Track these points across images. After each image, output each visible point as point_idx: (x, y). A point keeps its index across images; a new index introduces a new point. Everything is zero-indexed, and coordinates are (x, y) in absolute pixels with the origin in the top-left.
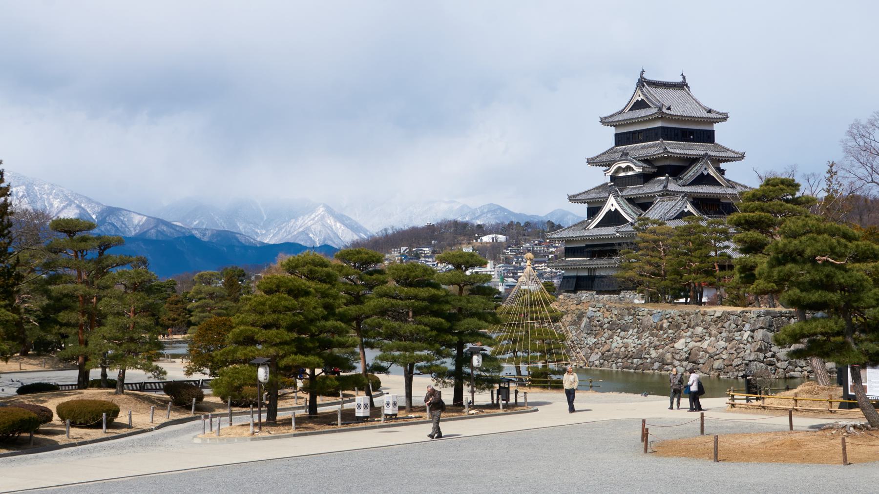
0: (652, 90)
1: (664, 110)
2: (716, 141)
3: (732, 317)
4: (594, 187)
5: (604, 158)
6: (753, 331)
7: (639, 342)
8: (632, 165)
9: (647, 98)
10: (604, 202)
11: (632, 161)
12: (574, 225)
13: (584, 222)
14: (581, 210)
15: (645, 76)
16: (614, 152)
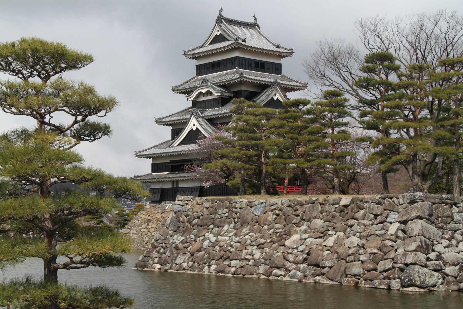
0: (230, 27)
1: (240, 41)
2: (283, 73)
3: (366, 205)
4: (178, 111)
5: (187, 86)
6: (405, 222)
7: (237, 239)
8: (211, 90)
9: (225, 32)
10: (185, 123)
11: (211, 87)
12: (160, 144)
13: (168, 141)
14: (167, 132)
15: (223, 14)
16: (196, 81)
